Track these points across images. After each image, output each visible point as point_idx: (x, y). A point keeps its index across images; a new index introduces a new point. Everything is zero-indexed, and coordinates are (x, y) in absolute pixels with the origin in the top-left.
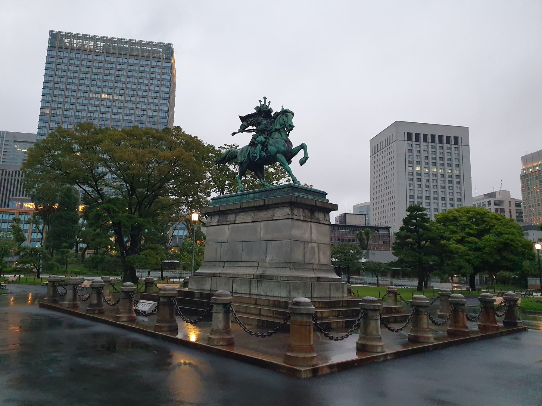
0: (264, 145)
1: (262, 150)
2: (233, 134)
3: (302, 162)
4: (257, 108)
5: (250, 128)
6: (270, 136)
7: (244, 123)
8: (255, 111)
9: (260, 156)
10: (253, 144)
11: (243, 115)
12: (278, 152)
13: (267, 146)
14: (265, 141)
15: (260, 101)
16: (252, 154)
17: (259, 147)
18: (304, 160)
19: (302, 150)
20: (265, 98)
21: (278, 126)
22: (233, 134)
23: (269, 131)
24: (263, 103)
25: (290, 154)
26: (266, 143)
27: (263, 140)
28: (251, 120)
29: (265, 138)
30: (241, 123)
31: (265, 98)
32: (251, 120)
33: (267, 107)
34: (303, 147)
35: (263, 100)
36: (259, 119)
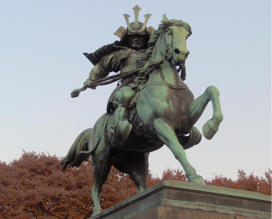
0: (130, 107)
1: (127, 116)
2: (75, 94)
4: (121, 29)
5: (112, 74)
7: (97, 66)
11: (92, 50)
12: (156, 115)
14: (133, 97)
15: (126, 16)
17: (121, 111)
20: (137, 9)
22: (75, 94)
23: (143, 73)
24: (132, 20)
26: (134, 100)
28: (110, 57)
29: (134, 89)
31: (137, 9)
32: (110, 57)
33: (141, 24)
35: (132, 13)
36: (123, 53)
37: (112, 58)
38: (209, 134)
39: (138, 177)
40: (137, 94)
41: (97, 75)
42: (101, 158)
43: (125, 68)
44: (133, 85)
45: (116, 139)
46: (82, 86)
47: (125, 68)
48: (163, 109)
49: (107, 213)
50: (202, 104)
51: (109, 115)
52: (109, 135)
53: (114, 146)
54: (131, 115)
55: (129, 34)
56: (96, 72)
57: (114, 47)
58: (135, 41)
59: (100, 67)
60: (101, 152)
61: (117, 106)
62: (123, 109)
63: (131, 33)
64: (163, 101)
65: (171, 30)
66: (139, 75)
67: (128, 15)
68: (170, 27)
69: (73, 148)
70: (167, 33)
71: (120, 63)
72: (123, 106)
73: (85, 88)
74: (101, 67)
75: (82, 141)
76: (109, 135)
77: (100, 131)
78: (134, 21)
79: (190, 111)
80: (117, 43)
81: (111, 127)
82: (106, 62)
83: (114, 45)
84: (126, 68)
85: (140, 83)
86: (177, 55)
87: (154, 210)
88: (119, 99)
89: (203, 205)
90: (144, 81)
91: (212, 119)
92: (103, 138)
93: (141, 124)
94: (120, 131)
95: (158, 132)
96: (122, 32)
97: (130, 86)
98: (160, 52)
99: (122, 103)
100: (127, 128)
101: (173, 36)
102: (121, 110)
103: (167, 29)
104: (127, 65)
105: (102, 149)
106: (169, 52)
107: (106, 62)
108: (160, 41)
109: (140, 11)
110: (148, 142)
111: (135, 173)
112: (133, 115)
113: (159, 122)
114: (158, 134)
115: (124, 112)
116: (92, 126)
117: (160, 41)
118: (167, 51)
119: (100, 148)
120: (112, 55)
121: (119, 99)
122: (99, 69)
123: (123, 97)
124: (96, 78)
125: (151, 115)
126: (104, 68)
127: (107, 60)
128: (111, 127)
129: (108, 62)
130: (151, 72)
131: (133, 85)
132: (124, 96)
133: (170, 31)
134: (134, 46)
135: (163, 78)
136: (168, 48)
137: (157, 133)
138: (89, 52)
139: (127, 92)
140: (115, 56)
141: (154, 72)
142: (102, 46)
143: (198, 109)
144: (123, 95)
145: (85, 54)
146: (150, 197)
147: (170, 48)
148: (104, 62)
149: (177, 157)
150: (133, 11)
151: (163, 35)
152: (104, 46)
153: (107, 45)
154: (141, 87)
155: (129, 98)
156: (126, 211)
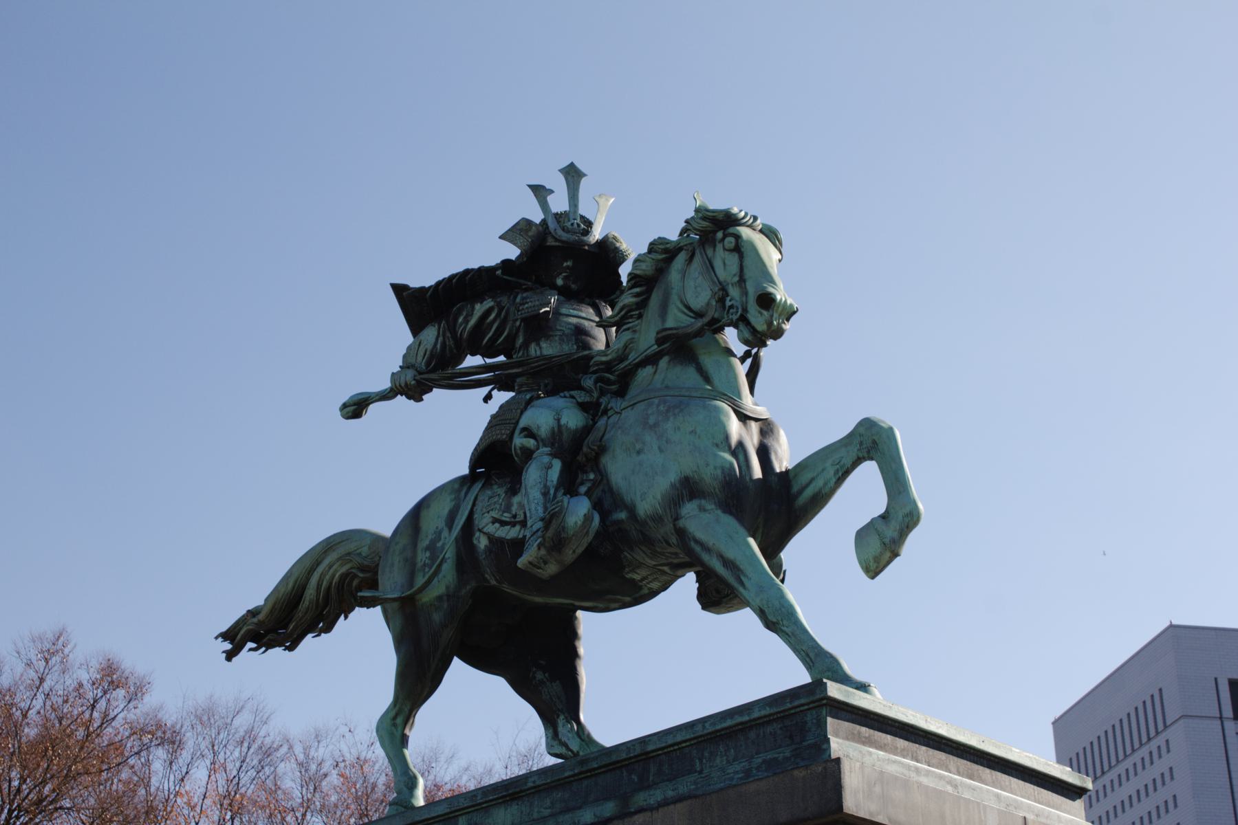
0: (580, 458)
1: (569, 484)
2: (356, 408)
3: (882, 543)
6: (621, 393)
7: (430, 334)
8: (512, 252)
9: (552, 518)
10: (495, 460)
11: (424, 277)
12: (689, 489)
13: (595, 461)
14: (587, 430)
15: (540, 191)
16: (488, 528)
18: (890, 532)
19: (869, 472)
20: (572, 174)
21: (676, 319)
22: (356, 408)
24: (559, 203)
25: (780, 505)
27: (573, 419)
28: (479, 309)
29: (583, 407)
30: (408, 338)
31: (572, 174)
32: (479, 309)
34: (871, 443)
35: (558, 185)
37: (487, 313)
38: (877, 559)
39: (556, 688)
40: (602, 422)
41: (432, 355)
42: (437, 617)
43: (538, 345)
44: (582, 397)
45: (543, 552)
46: (385, 384)
47: (538, 345)
48: (719, 472)
49: (538, 783)
50: (837, 471)
51: (478, 485)
52: (482, 543)
53: (493, 582)
54: (582, 484)
55: (551, 242)
56: (429, 347)
57: (498, 277)
58: (568, 267)
59: (444, 336)
60: (440, 598)
61: (528, 454)
62: (557, 465)
63: (556, 240)
64: (717, 445)
65: (738, 237)
66: (592, 369)
67: (543, 187)
68: (731, 230)
69: (290, 585)
70: (719, 247)
71: (518, 329)
72: (554, 455)
73: (386, 396)
74: (448, 334)
75: (330, 567)
76: (482, 543)
77: (439, 534)
78: (567, 208)
79: (795, 489)
80: (506, 263)
81: (495, 521)
82: (466, 321)
83: (499, 272)
84: (544, 345)
85: (602, 393)
86: (765, 313)
87: (825, 768)
88: (544, 432)
89: (928, 773)
90: (614, 387)
91: (884, 517)
92: (450, 553)
93: (623, 515)
94: (564, 528)
95: (697, 542)
96: (530, 234)
97: (572, 397)
98: (682, 302)
99: (552, 445)
100: (588, 518)
101: (741, 256)
102: (550, 467)
103: (720, 235)
104: (548, 337)
105: (447, 588)
106: (728, 303)
107: (452, 323)
108: (684, 274)
109: (584, 181)
110: (629, 576)
111: (540, 676)
112: (589, 485)
113: (702, 509)
114: (698, 549)
115: (562, 472)
116: (385, 523)
117: (684, 274)
118: (722, 301)
119: (438, 589)
120: (489, 303)
121: (544, 432)
122: (441, 339)
123: (559, 426)
124: (428, 364)
125: (673, 486)
126: (458, 341)
127: (470, 315)
128: (495, 521)
129: (472, 322)
130: (652, 360)
131: (582, 397)
132: (563, 422)
133: (732, 239)
134: (560, 282)
135: (707, 379)
136: (724, 289)
137: (692, 544)
138: (415, 283)
139: (550, 414)
140: (499, 304)
141: (663, 362)
142: (459, 268)
143: (825, 484)
144: (559, 420)
145: (400, 290)
146: (752, 735)
147: (734, 292)
148: (460, 320)
149: (770, 625)
150: (562, 178)
151: (697, 252)
152: (467, 272)
153: (476, 266)
154: (616, 404)
155: (576, 430)
156: (635, 777)
